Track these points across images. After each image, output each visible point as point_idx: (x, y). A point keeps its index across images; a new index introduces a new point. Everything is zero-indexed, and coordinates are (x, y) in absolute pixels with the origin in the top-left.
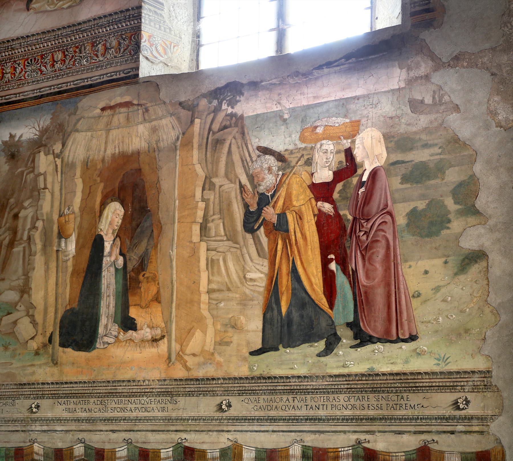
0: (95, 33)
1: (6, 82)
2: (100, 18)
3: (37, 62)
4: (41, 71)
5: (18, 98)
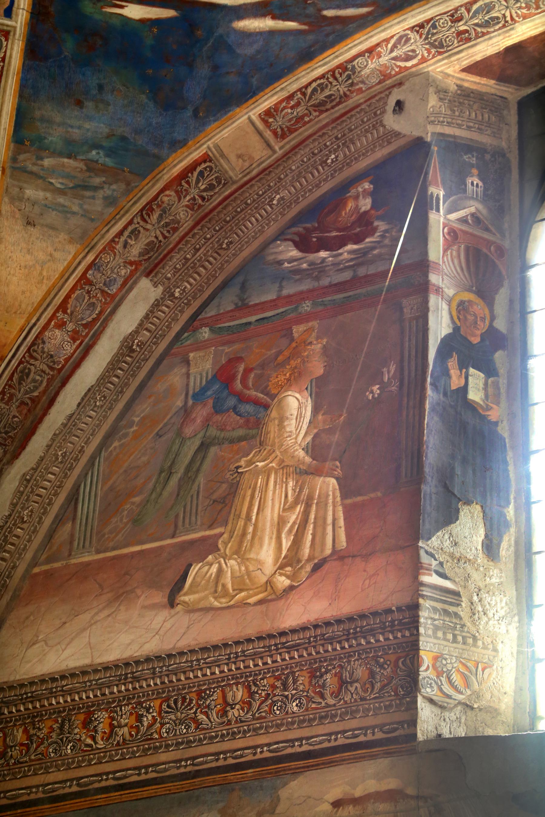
0: (318, 653)
1: (118, 744)
2: (328, 624)
3: (189, 704)
4: (198, 724)
5: (143, 777)
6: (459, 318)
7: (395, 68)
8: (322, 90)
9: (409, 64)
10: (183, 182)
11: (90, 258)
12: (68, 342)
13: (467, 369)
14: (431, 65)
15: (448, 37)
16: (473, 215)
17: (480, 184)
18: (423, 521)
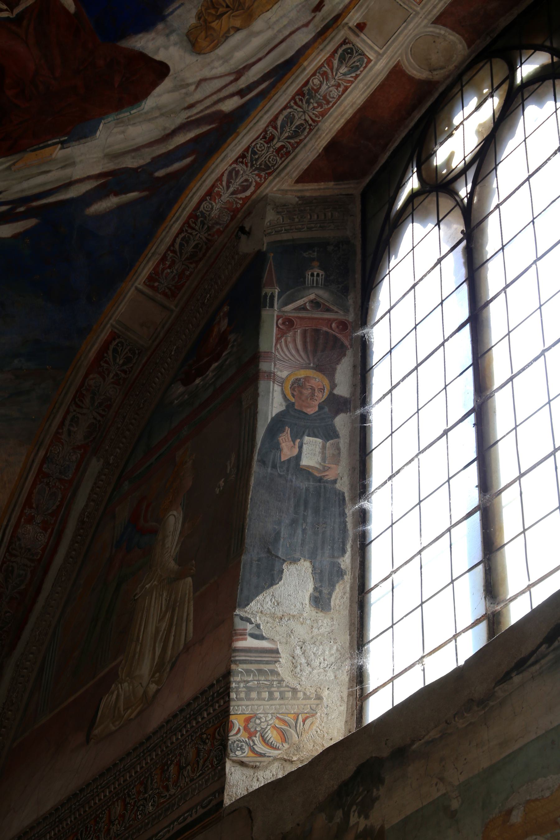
6: (293, 396)
7: (238, 201)
8: (187, 242)
9: (248, 193)
10: (101, 363)
11: (42, 453)
12: (41, 533)
13: (301, 437)
14: (266, 188)
15: (270, 158)
16: (311, 301)
17: (321, 273)
18: (242, 590)
